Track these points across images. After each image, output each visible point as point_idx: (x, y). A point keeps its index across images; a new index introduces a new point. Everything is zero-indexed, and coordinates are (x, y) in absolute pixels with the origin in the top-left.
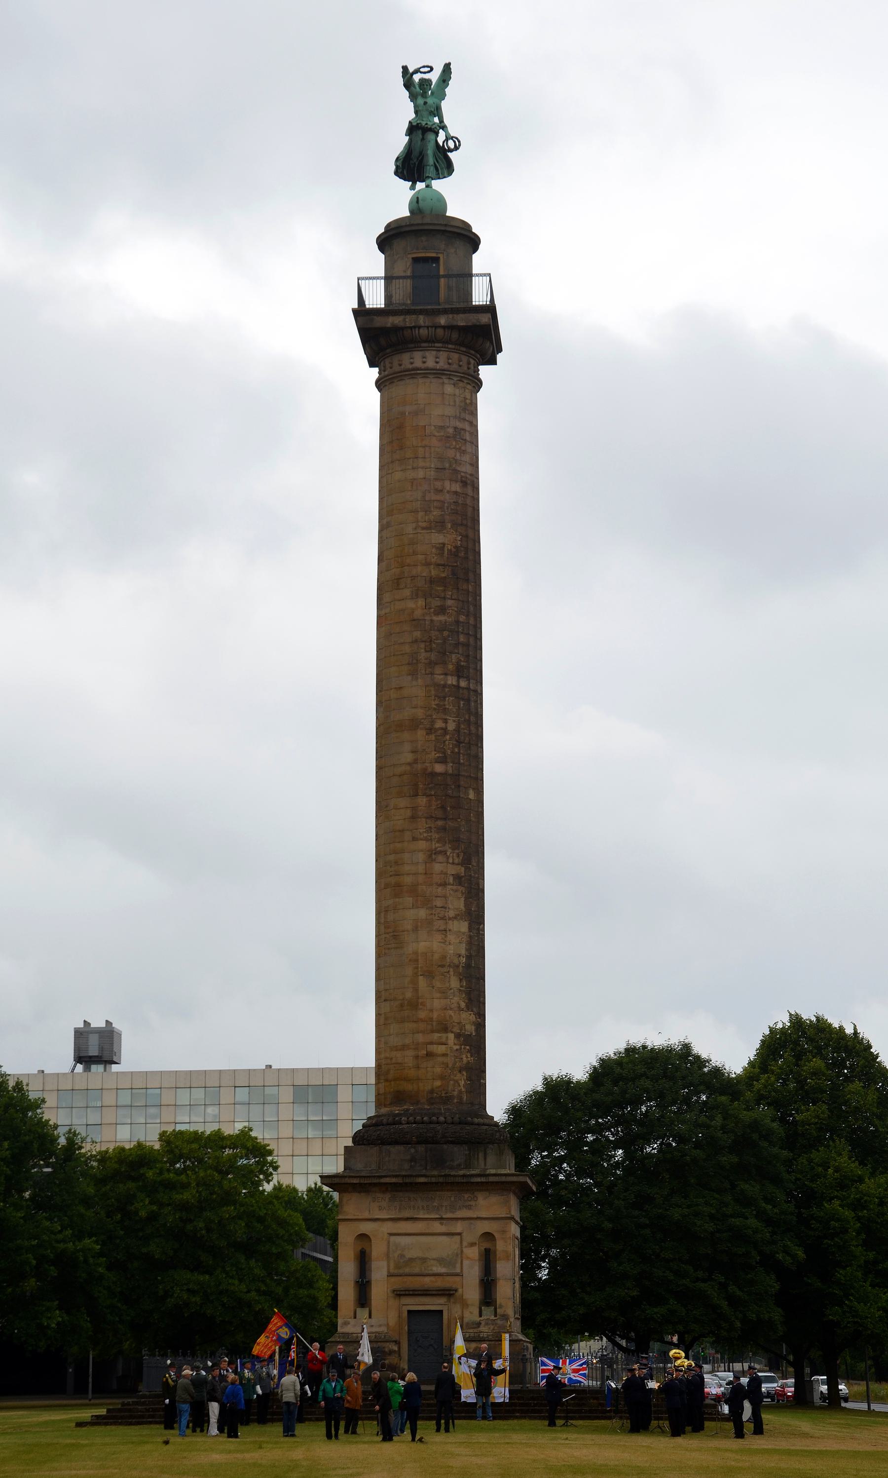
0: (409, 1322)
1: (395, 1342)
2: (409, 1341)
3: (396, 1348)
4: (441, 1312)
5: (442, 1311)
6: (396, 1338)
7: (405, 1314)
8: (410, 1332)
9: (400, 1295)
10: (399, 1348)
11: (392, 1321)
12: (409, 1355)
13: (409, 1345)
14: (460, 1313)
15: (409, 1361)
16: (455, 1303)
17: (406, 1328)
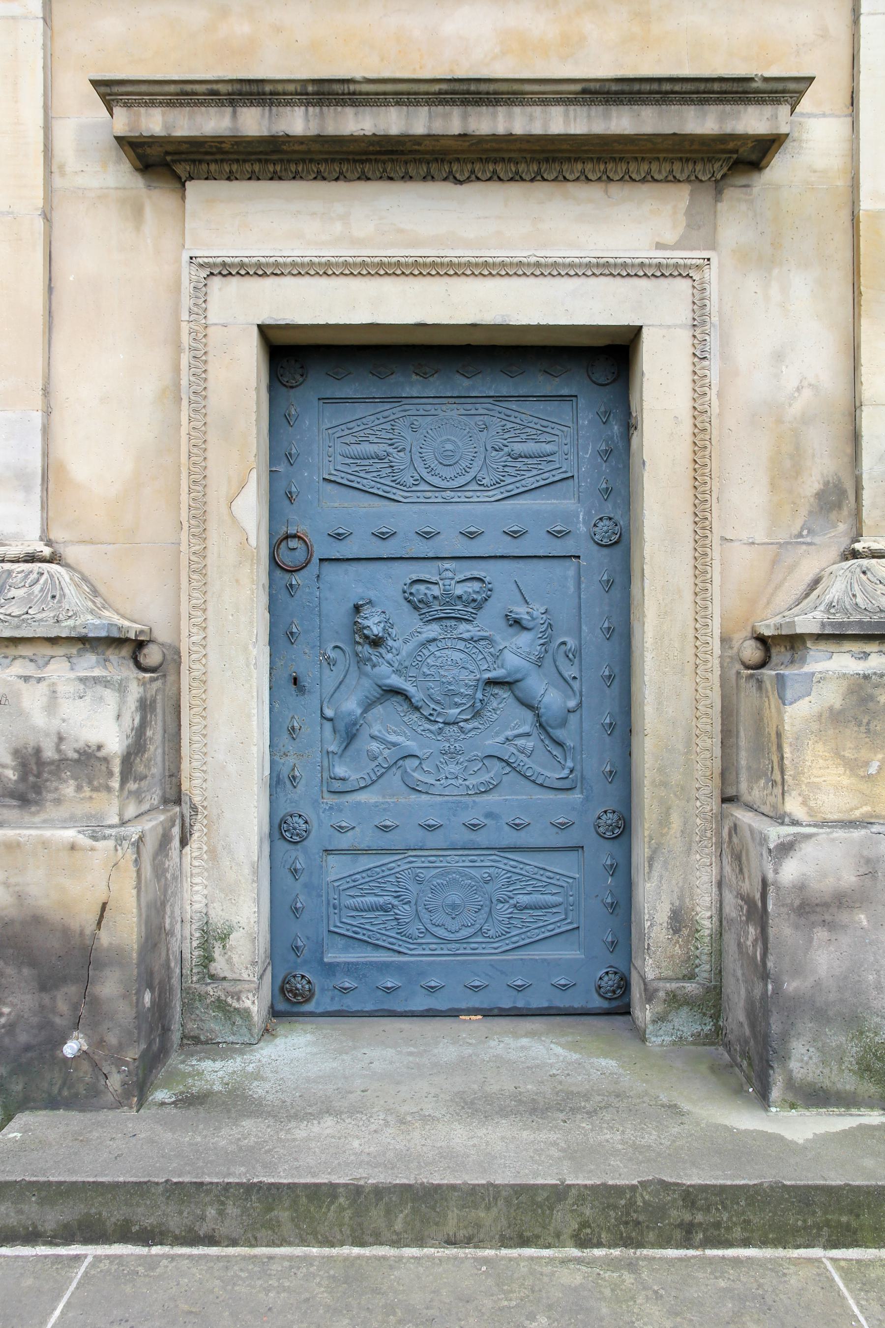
0: (281, 454)
1: (134, 646)
2: (281, 637)
3: (96, 715)
4: (611, 356)
5: (611, 356)
6: (139, 604)
7: (242, 369)
8: (287, 557)
9: (163, 163)
10: (161, 726)
11: (105, 451)
12: (279, 782)
13: (287, 684)
14: (815, 363)
15: (283, 831)
16: (765, 259)
17: (249, 511)
